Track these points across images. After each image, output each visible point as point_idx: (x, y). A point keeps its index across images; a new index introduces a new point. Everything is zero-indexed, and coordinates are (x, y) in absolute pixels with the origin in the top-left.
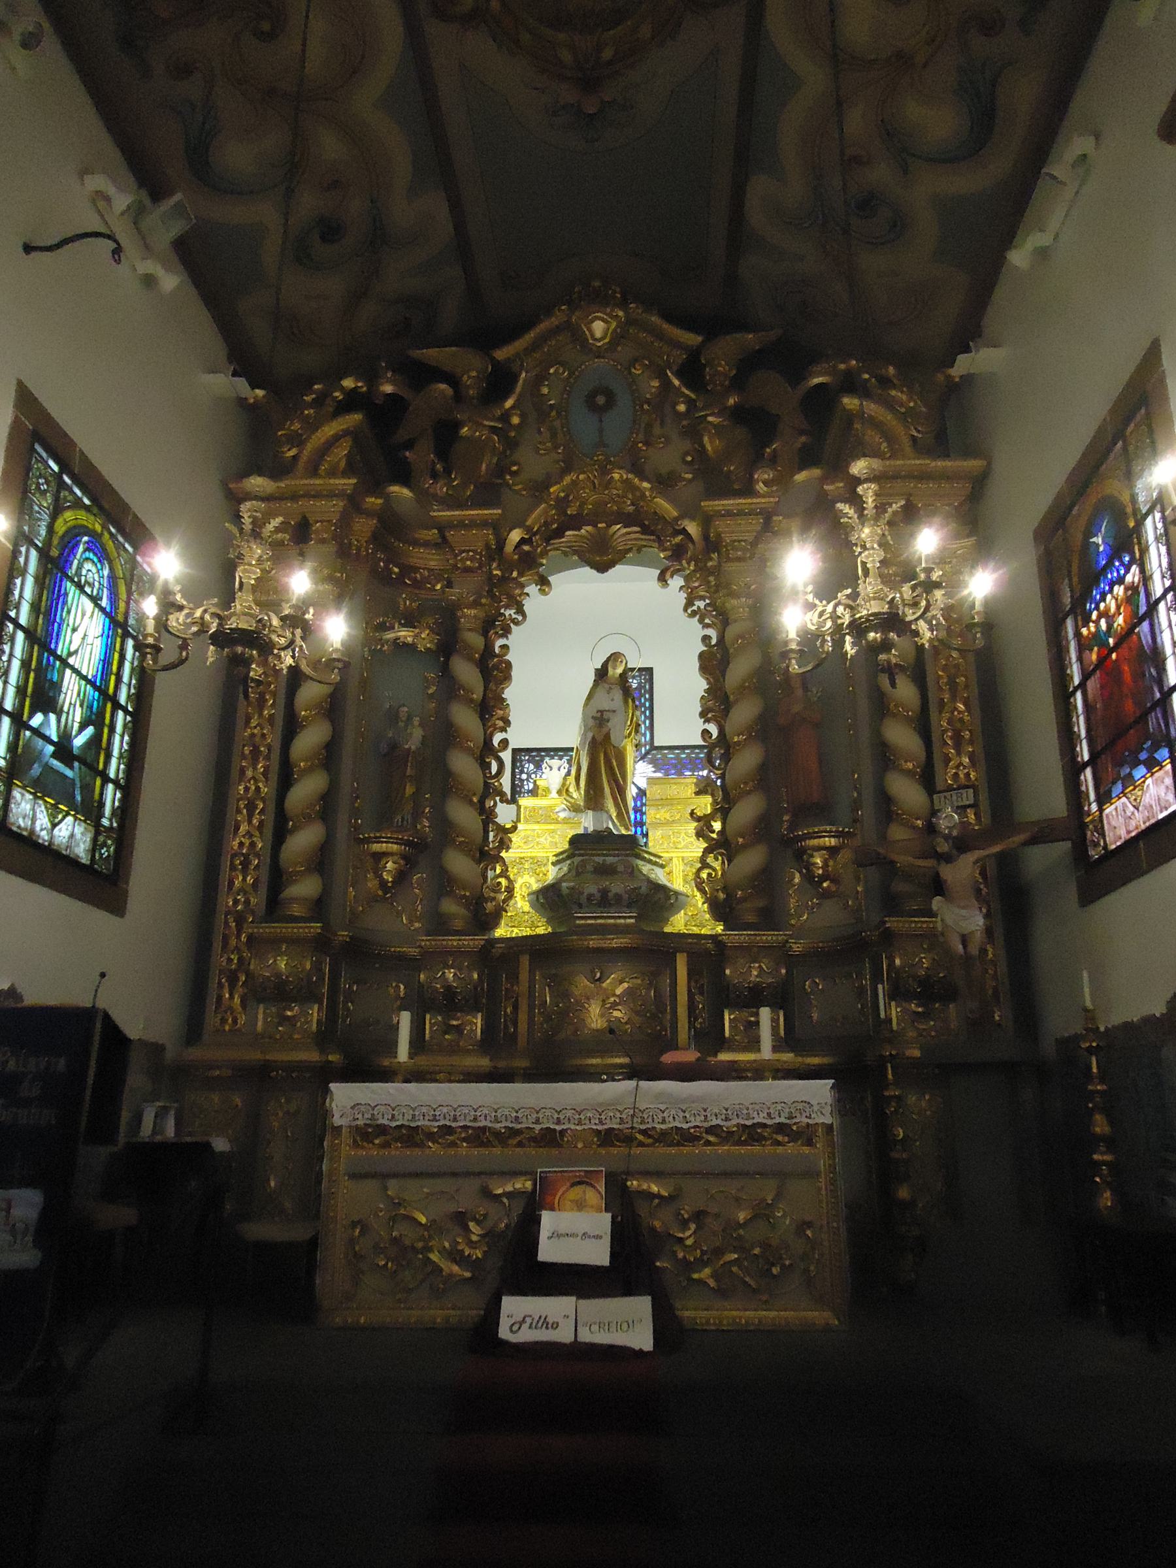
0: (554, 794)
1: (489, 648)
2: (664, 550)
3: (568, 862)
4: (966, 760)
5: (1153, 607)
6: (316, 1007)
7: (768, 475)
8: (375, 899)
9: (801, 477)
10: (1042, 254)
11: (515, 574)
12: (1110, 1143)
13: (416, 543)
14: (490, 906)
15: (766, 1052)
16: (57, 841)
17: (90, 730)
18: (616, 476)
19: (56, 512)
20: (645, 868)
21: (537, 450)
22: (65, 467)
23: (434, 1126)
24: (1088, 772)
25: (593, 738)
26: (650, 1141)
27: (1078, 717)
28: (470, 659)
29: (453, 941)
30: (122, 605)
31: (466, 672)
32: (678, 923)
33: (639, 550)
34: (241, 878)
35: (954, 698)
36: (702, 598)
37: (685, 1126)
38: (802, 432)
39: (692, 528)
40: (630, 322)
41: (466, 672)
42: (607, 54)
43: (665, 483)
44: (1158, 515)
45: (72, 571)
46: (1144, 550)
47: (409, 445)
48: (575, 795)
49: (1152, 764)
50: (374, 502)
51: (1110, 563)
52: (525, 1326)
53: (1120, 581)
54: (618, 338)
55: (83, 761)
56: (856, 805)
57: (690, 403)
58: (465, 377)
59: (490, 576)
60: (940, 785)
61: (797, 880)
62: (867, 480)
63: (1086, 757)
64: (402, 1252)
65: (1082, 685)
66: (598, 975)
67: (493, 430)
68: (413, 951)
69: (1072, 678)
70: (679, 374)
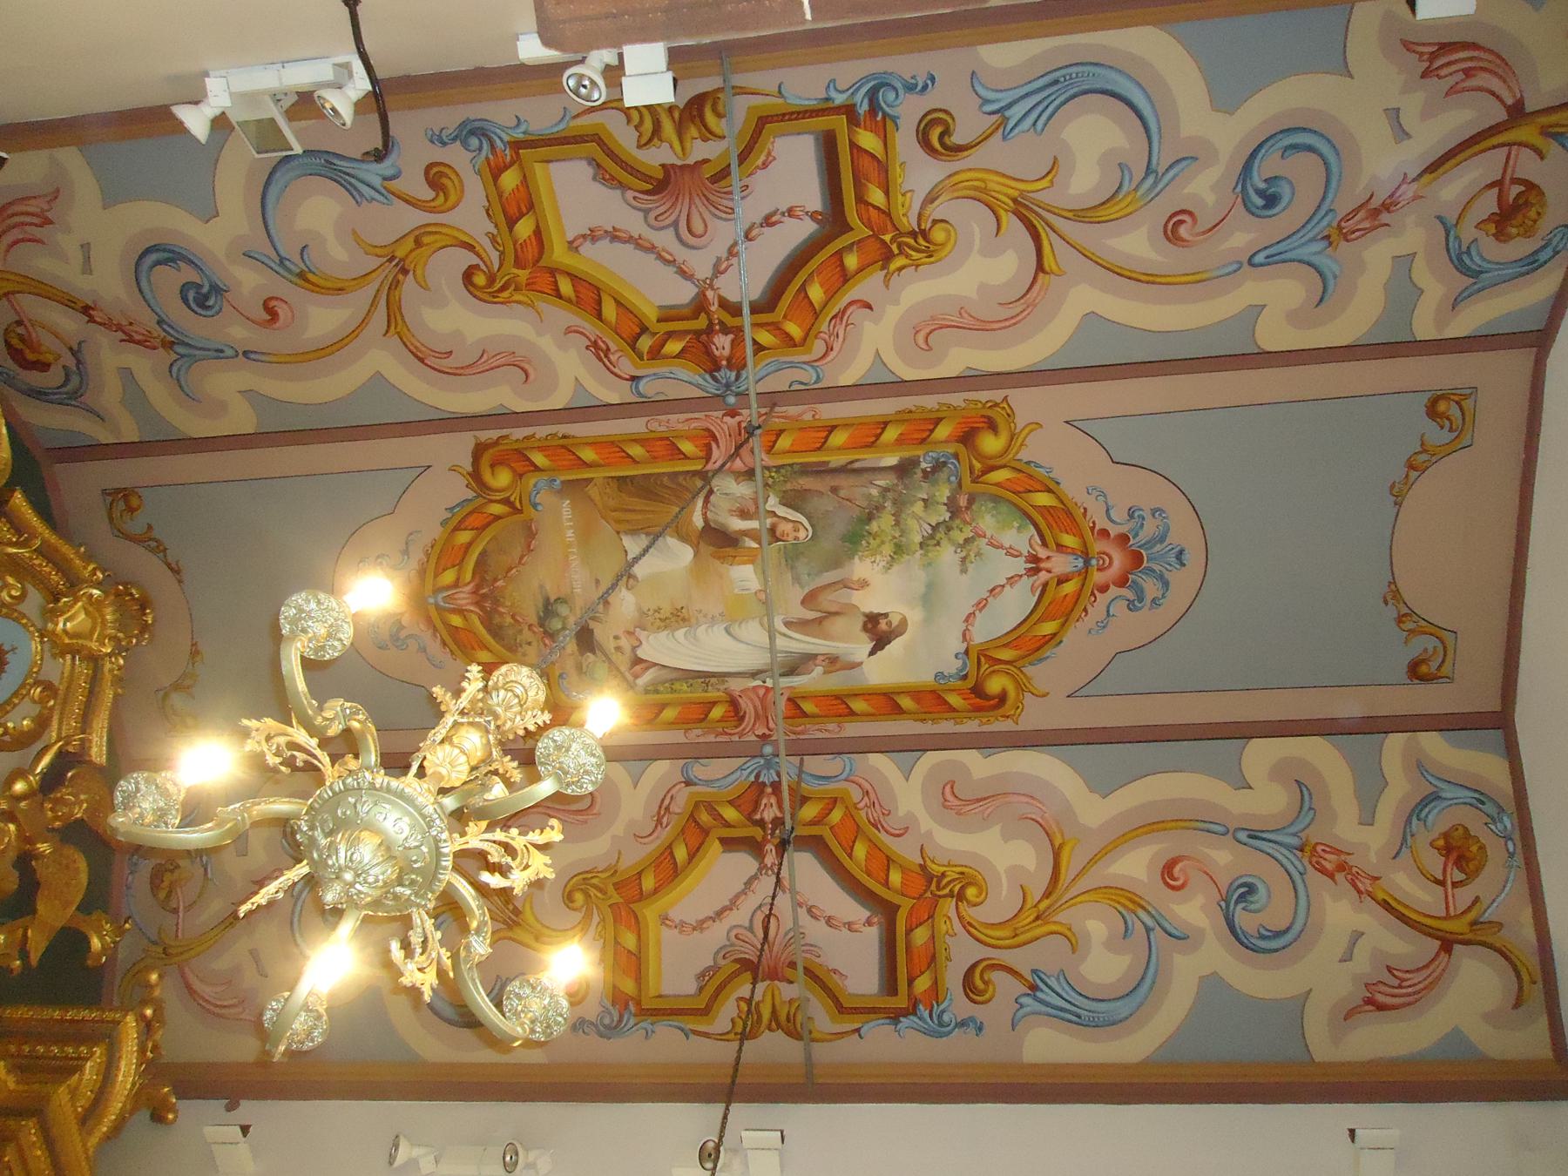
42: (456, 621)
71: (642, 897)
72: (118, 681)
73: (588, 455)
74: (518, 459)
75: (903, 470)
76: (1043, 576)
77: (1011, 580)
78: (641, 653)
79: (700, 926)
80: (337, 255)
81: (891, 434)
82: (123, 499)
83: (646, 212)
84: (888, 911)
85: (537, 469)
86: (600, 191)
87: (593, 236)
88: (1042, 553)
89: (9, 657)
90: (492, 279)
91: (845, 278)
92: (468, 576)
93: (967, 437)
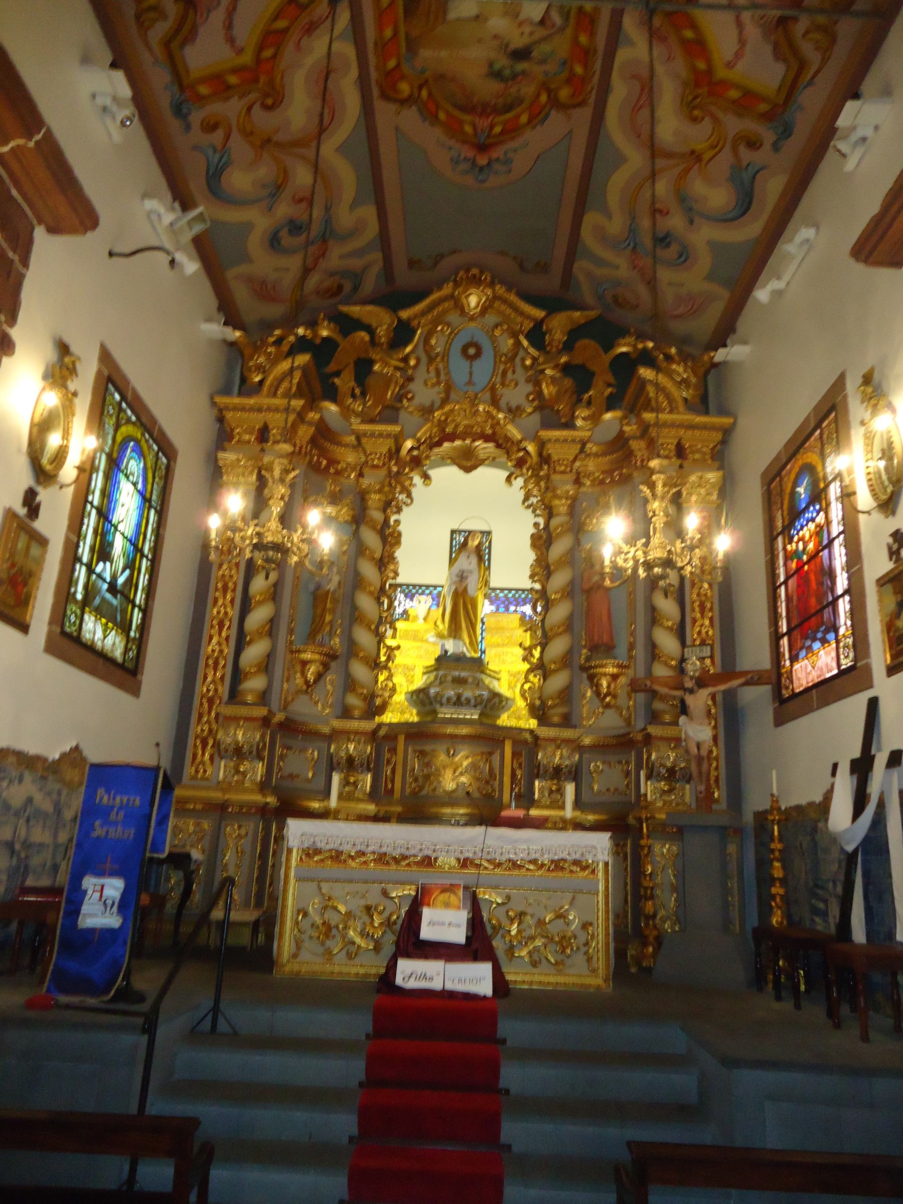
0: (421, 620)
2: (511, 460)
3: (435, 673)
4: (707, 622)
5: (831, 541)
6: (261, 764)
8: (299, 692)
9: (608, 416)
10: (778, 294)
11: (407, 470)
12: (783, 882)
13: (339, 444)
14: (378, 701)
15: (569, 812)
16: (106, 648)
17: (127, 572)
18: (481, 409)
19: (117, 427)
20: (487, 680)
21: (426, 384)
22: (123, 398)
23: (396, 854)
24: (786, 639)
25: (456, 590)
26: (492, 867)
27: (781, 603)
28: (374, 528)
29: (354, 725)
30: (149, 487)
32: (505, 720)
33: (494, 459)
34: (212, 673)
35: (703, 617)
36: (535, 496)
37: (515, 859)
38: (609, 385)
39: (531, 448)
40: (495, 297)
41: (371, 539)
42: (498, 129)
43: (514, 412)
44: (838, 483)
45: (123, 467)
46: (828, 505)
47: (338, 374)
48: (441, 627)
49: (824, 641)
50: (313, 416)
51: (807, 508)
52: (412, 979)
53: (813, 520)
54: (484, 311)
55: (122, 593)
56: (632, 647)
57: (535, 359)
58: (378, 331)
59: (390, 471)
60: (689, 641)
61: (589, 694)
62: (659, 472)
63: (785, 630)
64: (328, 929)
65: (785, 582)
66: (452, 752)
67: (397, 368)
68: (326, 730)
69: (779, 576)
70: (527, 337)
71: (710, 71)
72: (509, 290)
73: (388, 33)
74: (390, 79)
78: (538, 18)
79: (742, 42)
80: (265, 171)
83: (209, 11)
85: (398, 66)
86: (203, 33)
87: (231, 40)
89: (475, 340)
90: (267, 95)
92: (467, 118)
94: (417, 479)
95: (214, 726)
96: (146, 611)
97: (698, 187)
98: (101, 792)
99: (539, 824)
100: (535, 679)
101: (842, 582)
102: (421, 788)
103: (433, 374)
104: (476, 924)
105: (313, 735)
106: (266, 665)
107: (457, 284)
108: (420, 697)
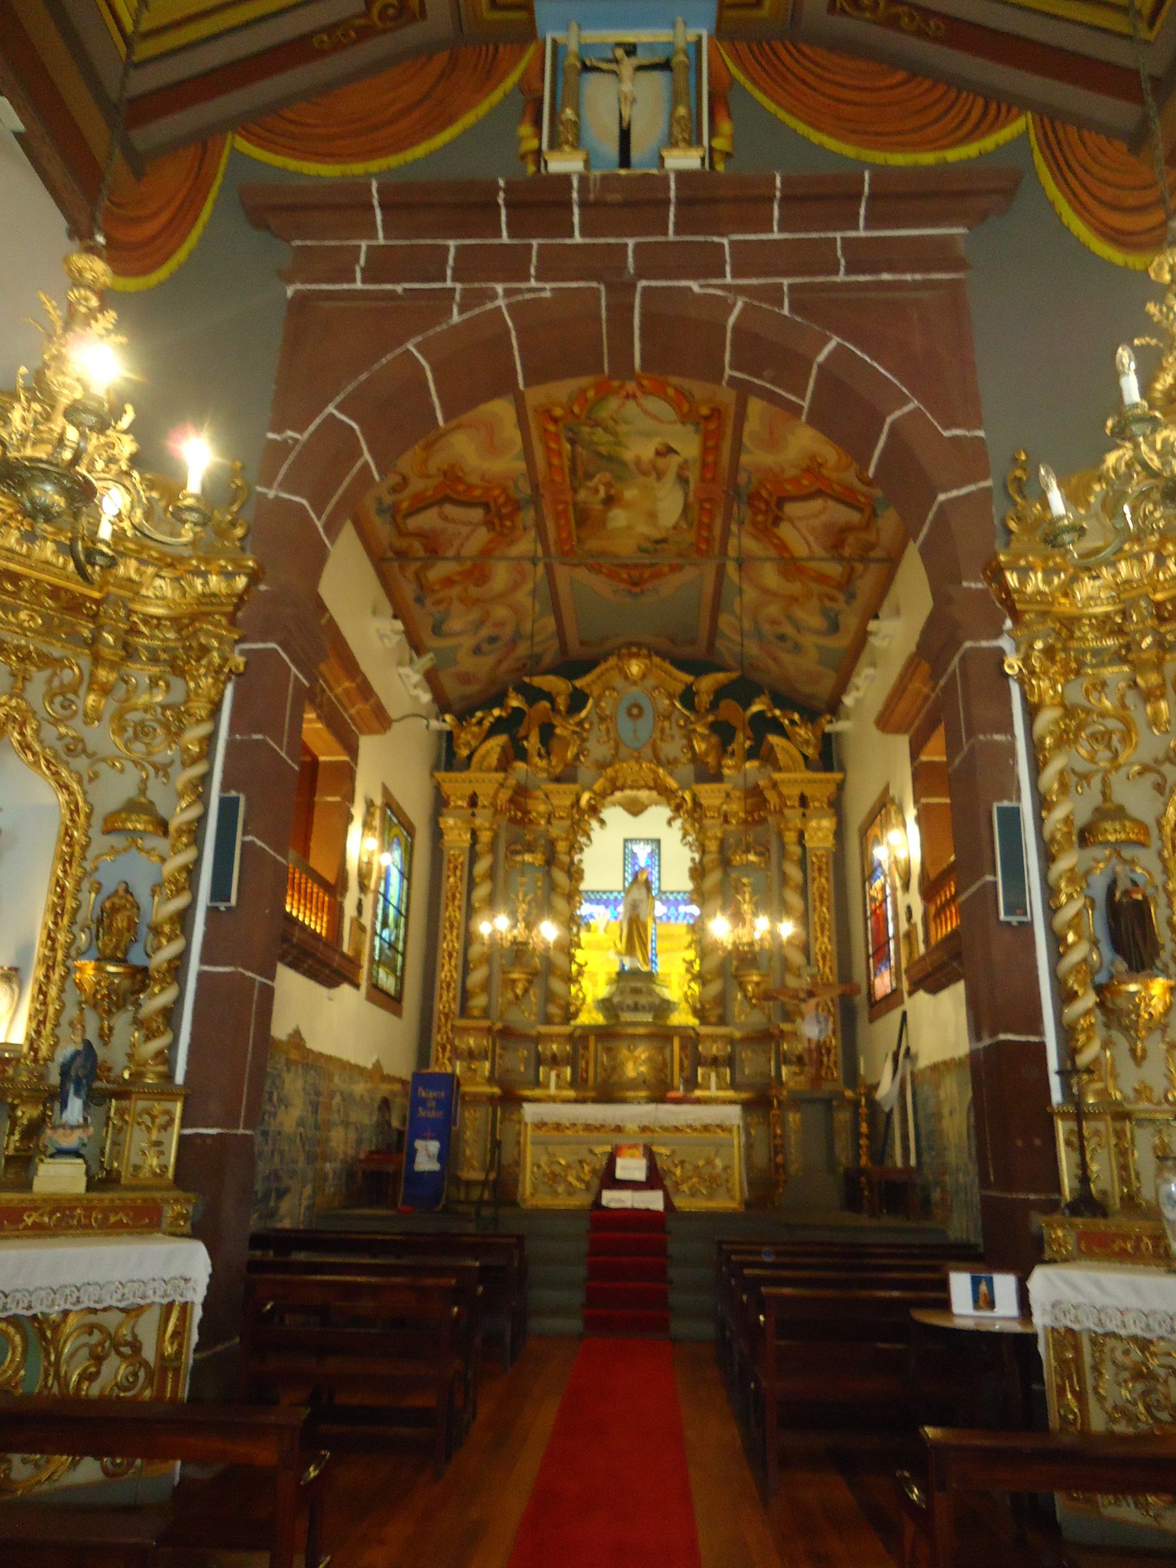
0: (601, 931)
1: (572, 862)
4: (826, 940)
7: (730, 762)
8: (510, 1003)
9: (748, 765)
10: (858, 701)
12: (868, 1137)
14: (572, 1009)
20: (657, 989)
21: (598, 741)
28: (562, 869)
31: (560, 877)
38: (749, 738)
39: (688, 796)
48: (619, 946)
54: (644, 676)
57: (687, 718)
67: (574, 732)
68: (534, 1032)
75: (572, 442)
76: (638, 394)
77: (639, 405)
80: (475, 615)
81: (553, 445)
82: (582, 643)
84: (819, 493)
88: (624, 393)
91: (470, 487)
93: (555, 420)
94: (595, 824)
95: (450, 1035)
96: (404, 955)
97: (799, 613)
98: (420, 1089)
99: (698, 1101)
100: (695, 987)
101: (891, 933)
102: (609, 1077)
103: (604, 732)
104: (652, 1168)
105: (524, 1038)
106: (486, 986)
107: (620, 657)
108: (606, 1005)
